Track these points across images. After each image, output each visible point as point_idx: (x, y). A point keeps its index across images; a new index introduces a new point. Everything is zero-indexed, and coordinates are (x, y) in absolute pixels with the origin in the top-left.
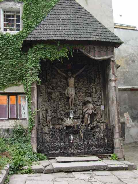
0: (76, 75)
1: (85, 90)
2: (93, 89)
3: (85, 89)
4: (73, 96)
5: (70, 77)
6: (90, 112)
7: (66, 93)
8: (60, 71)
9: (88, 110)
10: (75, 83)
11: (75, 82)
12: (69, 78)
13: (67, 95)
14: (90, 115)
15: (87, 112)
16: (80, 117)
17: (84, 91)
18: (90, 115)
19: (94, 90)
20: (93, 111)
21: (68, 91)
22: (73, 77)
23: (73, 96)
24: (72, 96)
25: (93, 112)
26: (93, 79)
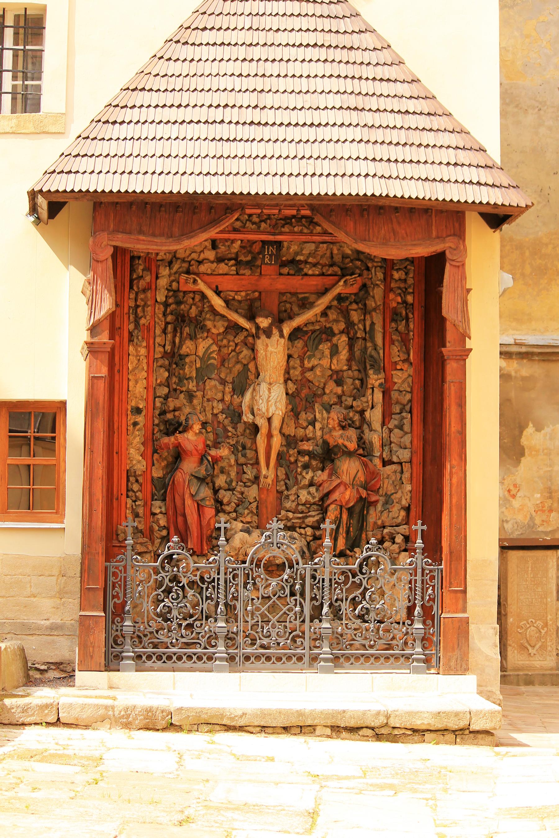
0: (297, 322)
1: (340, 397)
2: (373, 388)
3: (339, 390)
4: (276, 423)
5: (268, 333)
6: (347, 497)
7: (244, 408)
8: (222, 303)
9: (342, 488)
10: (288, 362)
11: (290, 356)
12: (263, 337)
13: (252, 417)
14: (350, 511)
15: (336, 496)
16: (310, 521)
17: (334, 399)
18: (350, 511)
19: (378, 396)
20: (364, 495)
21: (253, 398)
22: (282, 336)
23: (276, 423)
24: (269, 420)
25: (361, 497)
26: (379, 340)
